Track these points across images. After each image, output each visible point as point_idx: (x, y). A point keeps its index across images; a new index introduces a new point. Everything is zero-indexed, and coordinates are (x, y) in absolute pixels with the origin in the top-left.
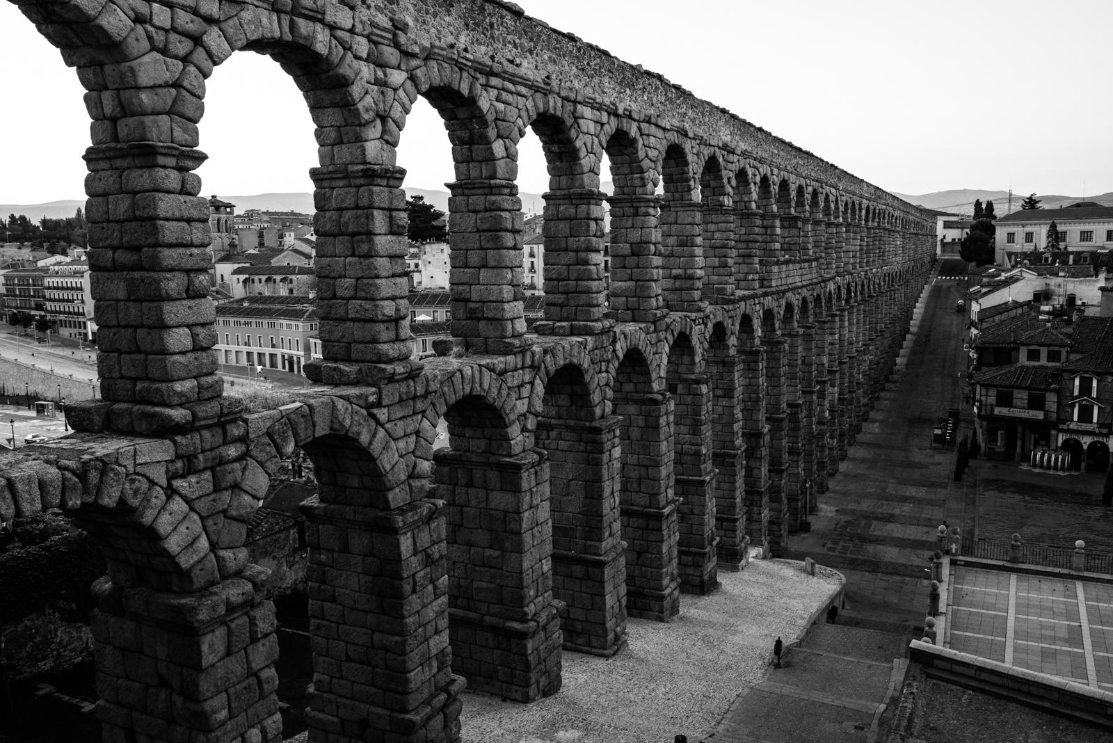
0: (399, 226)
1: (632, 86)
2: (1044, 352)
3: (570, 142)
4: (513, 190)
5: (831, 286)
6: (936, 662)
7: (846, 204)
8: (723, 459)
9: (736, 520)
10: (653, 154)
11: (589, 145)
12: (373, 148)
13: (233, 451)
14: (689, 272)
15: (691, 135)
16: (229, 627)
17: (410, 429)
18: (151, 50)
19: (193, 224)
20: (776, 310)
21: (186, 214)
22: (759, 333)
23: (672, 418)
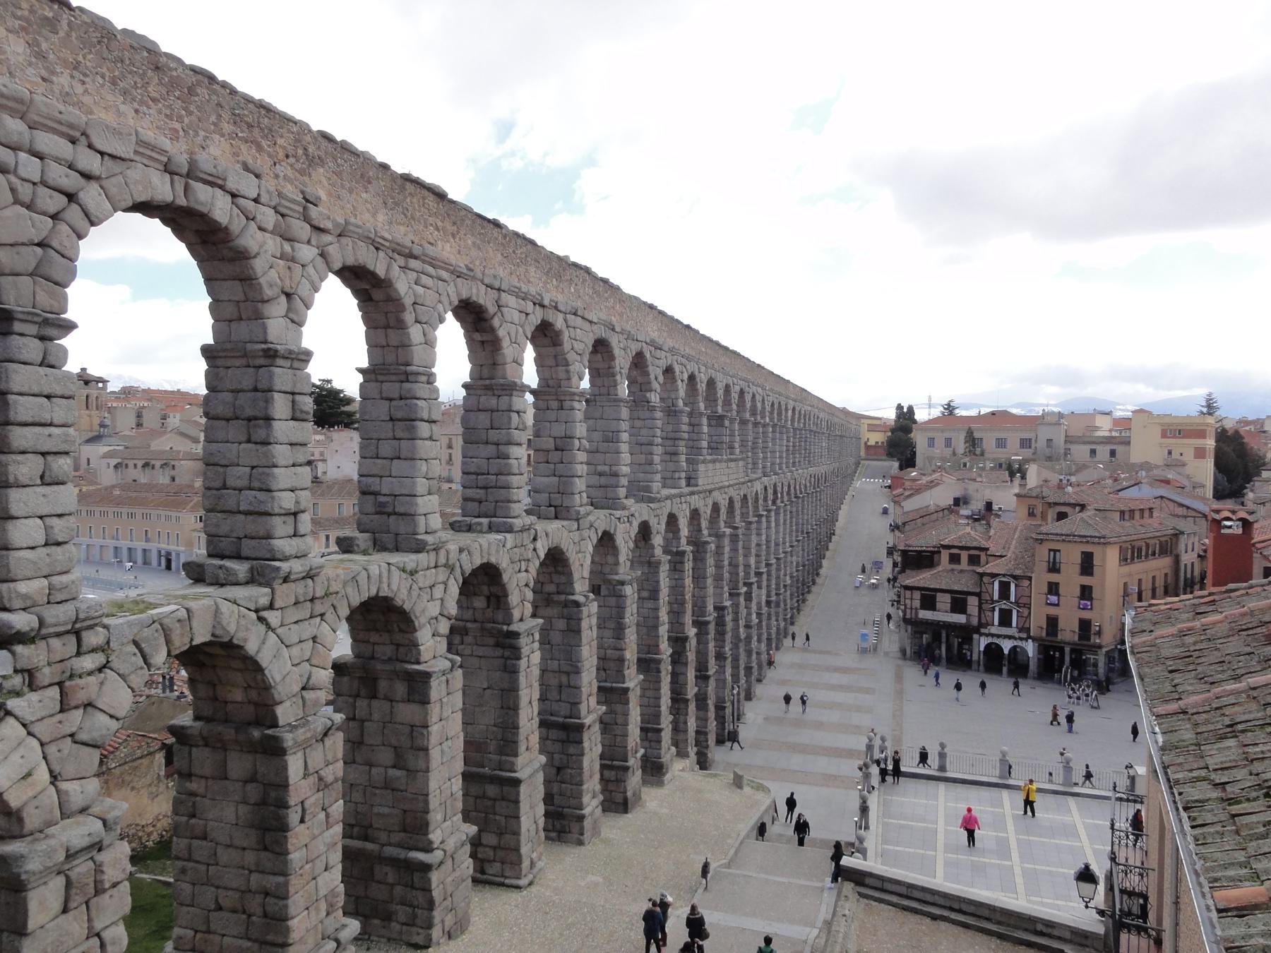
0: (302, 411)
1: (559, 277)
2: (964, 556)
3: (493, 330)
4: (431, 378)
5: (758, 487)
6: (868, 881)
7: (773, 405)
8: (647, 665)
9: (660, 731)
10: (579, 346)
11: (513, 335)
12: (276, 327)
13: (88, 662)
14: (614, 468)
15: (618, 329)
16: (67, 877)
17: (307, 634)
18: (15, 203)
19: (54, 400)
20: (701, 512)
21: (46, 391)
22: (684, 532)
23: (594, 621)
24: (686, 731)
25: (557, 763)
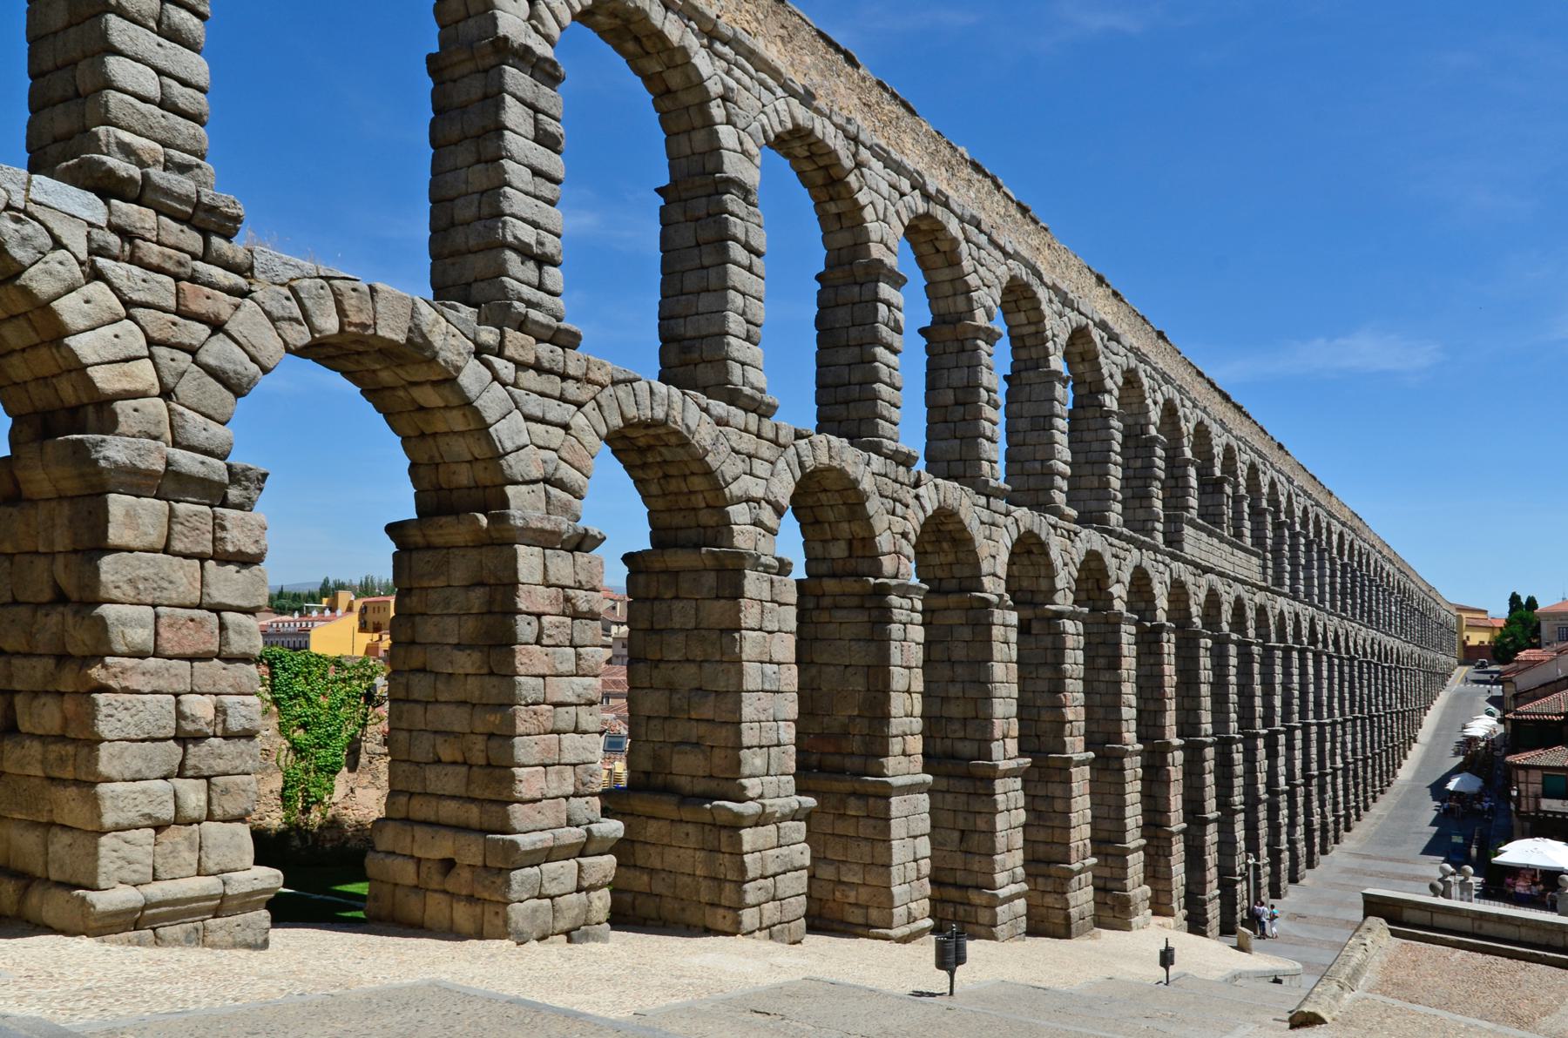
20: (1191, 588)
24: (1169, 878)
25: (961, 824)
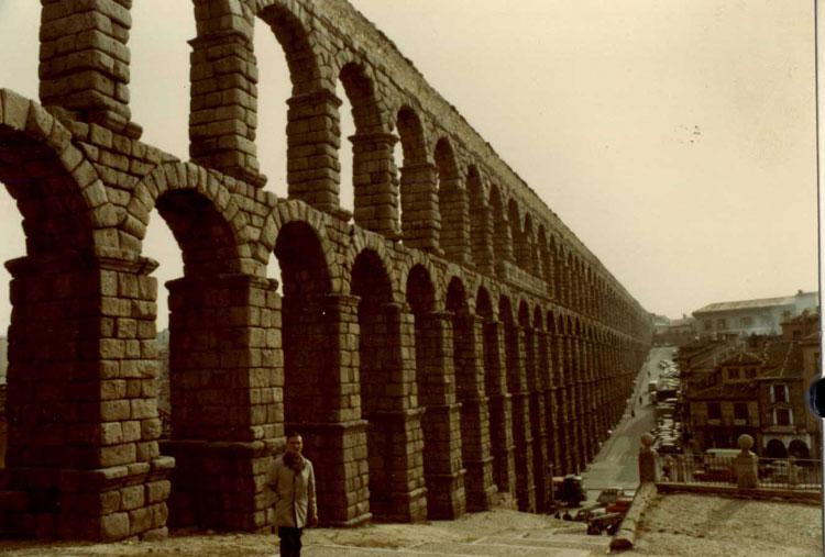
2: (742, 372)
3: (307, 48)
10: (390, 104)
20: (512, 301)
22: (496, 310)
